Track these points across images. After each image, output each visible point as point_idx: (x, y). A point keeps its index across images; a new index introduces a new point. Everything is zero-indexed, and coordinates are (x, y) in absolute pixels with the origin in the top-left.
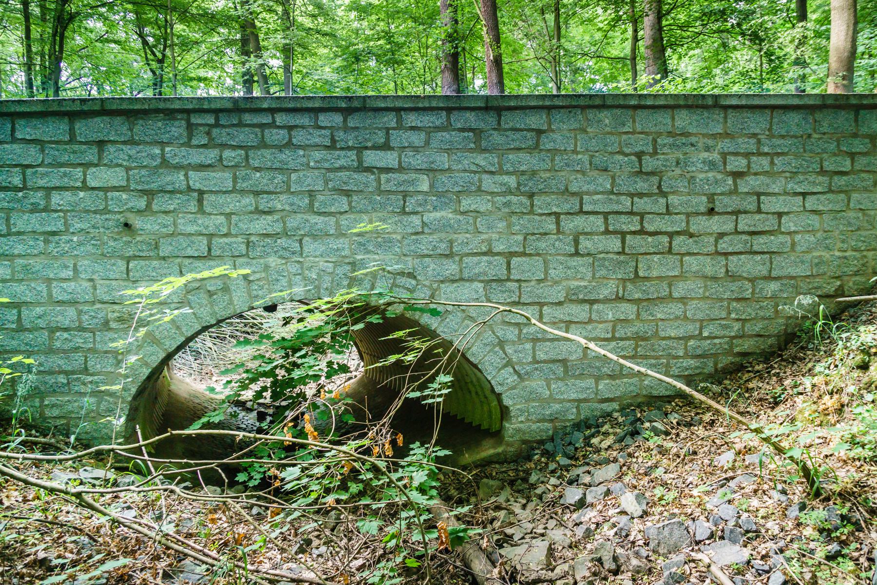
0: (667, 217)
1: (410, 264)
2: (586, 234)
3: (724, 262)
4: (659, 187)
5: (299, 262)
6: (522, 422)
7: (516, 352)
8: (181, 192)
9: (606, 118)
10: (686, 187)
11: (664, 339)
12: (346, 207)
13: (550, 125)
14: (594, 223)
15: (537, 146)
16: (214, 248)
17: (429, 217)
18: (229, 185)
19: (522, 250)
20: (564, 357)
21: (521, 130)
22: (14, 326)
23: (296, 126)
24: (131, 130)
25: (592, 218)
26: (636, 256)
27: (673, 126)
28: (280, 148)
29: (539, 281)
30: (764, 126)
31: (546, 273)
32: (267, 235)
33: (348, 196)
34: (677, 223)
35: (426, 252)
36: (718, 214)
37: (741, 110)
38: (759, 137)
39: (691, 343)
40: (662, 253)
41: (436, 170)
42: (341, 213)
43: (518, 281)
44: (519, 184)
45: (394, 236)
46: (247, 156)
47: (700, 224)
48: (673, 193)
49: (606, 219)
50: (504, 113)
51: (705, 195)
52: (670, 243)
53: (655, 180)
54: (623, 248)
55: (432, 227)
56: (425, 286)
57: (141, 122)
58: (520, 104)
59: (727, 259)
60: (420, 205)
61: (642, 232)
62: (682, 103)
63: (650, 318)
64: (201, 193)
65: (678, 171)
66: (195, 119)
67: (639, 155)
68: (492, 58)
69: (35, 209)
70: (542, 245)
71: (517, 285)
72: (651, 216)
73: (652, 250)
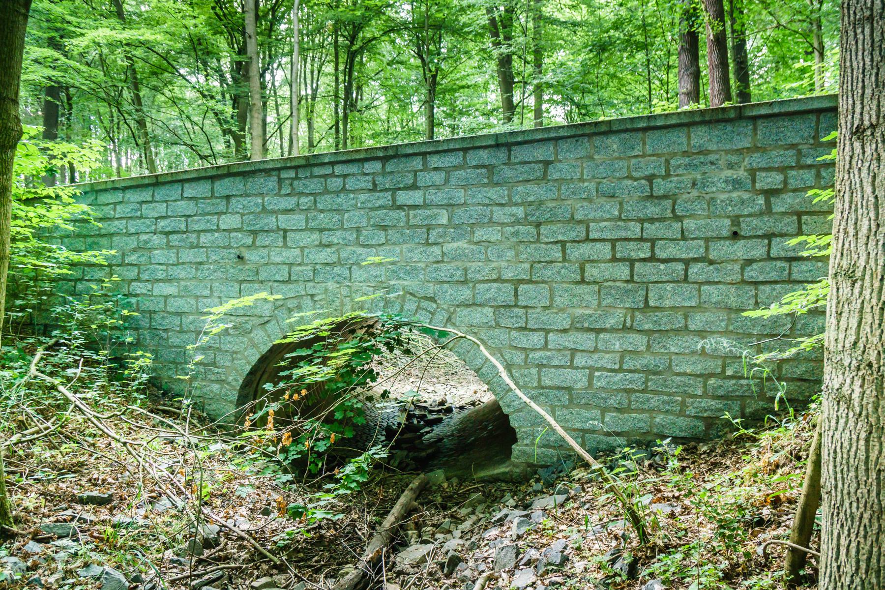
0: (682, 243)
1: (431, 289)
2: (592, 261)
3: (753, 293)
4: (673, 211)
5: (348, 286)
6: (527, 445)
7: (522, 375)
8: (273, 231)
9: (614, 143)
10: (704, 210)
11: (678, 374)
12: (383, 240)
13: (556, 155)
14: (600, 251)
15: (545, 177)
16: (293, 274)
17: (447, 247)
18: (303, 225)
19: (529, 277)
20: (568, 385)
21: (530, 163)
22: (178, 329)
23: (349, 175)
24: (245, 186)
25: (598, 245)
26: (646, 285)
27: (689, 144)
28: (337, 193)
29: (545, 308)
30: (806, 135)
31: (552, 299)
32: (327, 264)
33: (386, 230)
34: (695, 249)
35: (445, 279)
36: (744, 238)
37: (775, 119)
38: (800, 147)
39: (712, 381)
40: (678, 282)
41: (454, 205)
42: (380, 245)
43: (525, 307)
44: (526, 215)
45: (419, 265)
46: (315, 201)
47: (719, 250)
48: (690, 216)
49: (614, 247)
50: (513, 148)
51: (728, 217)
52: (686, 271)
53: (668, 203)
54: (632, 276)
55: (450, 256)
56: (443, 309)
57: (251, 180)
58: (527, 138)
59: (756, 289)
60: (441, 236)
61: (653, 259)
62: (697, 119)
63: (663, 350)
64: (285, 231)
65: (695, 193)
66: (284, 175)
67: (650, 179)
68: (712, 37)
69: (192, 247)
70: (548, 273)
71: (523, 311)
72: (662, 242)
73: (665, 278)
